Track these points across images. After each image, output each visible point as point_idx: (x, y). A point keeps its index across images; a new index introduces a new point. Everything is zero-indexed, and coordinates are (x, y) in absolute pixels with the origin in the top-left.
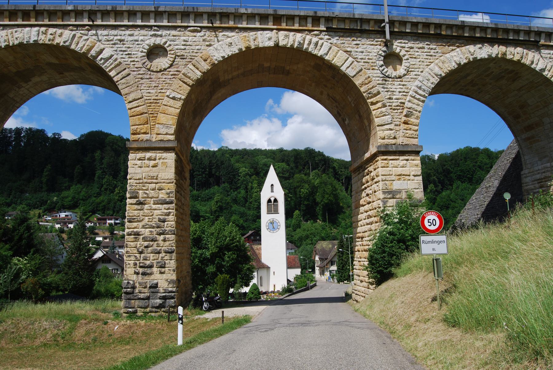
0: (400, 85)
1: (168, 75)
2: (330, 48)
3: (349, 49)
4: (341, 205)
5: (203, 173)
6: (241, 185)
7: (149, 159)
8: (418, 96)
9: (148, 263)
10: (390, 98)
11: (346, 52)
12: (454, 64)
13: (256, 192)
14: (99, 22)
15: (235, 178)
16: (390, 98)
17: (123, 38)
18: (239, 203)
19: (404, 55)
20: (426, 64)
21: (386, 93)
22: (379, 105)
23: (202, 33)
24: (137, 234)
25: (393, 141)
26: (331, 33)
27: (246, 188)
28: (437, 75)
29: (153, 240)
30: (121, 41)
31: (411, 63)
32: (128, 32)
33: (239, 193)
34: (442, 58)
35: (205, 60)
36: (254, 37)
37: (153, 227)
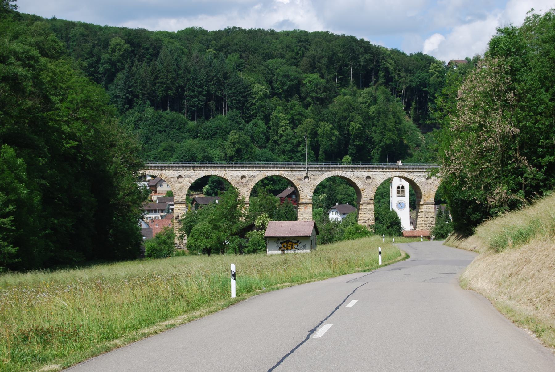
4: (405, 142)
5: (200, 93)
6: (256, 113)
13: (283, 126)
14: (414, 171)
15: (247, 101)
18: (257, 142)
27: (267, 119)
33: (256, 125)
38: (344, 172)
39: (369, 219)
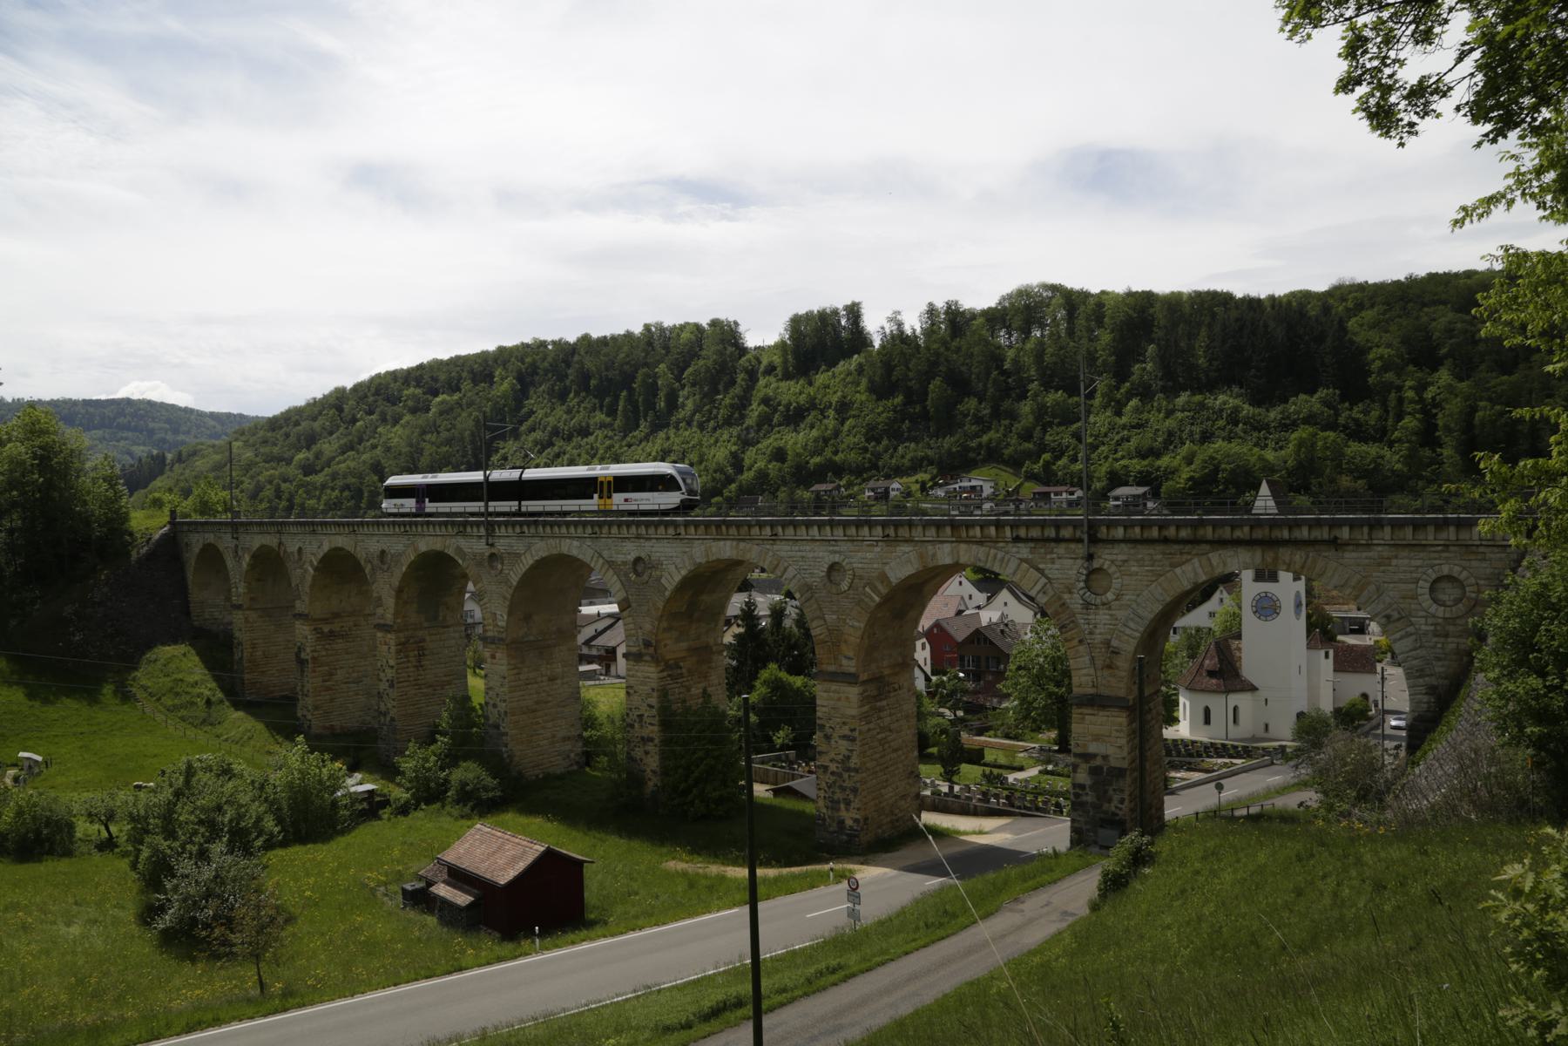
0: (1105, 614)
1: (847, 598)
2: (1019, 565)
3: (1041, 566)
7: (834, 692)
8: (1128, 631)
9: (836, 797)
10: (1091, 633)
11: (1038, 570)
12: (1185, 583)
16: (1091, 633)
17: (804, 554)
19: (1115, 572)
20: (1145, 583)
21: (1086, 626)
22: (1075, 642)
23: (878, 549)
24: (826, 768)
25: (1091, 691)
26: (1019, 545)
28: (1158, 600)
29: (840, 775)
30: (803, 557)
31: (1125, 582)
32: (808, 548)
34: (1168, 575)
35: (882, 582)
36: (930, 553)
37: (837, 762)
38: (576, 543)
39: (641, 716)
